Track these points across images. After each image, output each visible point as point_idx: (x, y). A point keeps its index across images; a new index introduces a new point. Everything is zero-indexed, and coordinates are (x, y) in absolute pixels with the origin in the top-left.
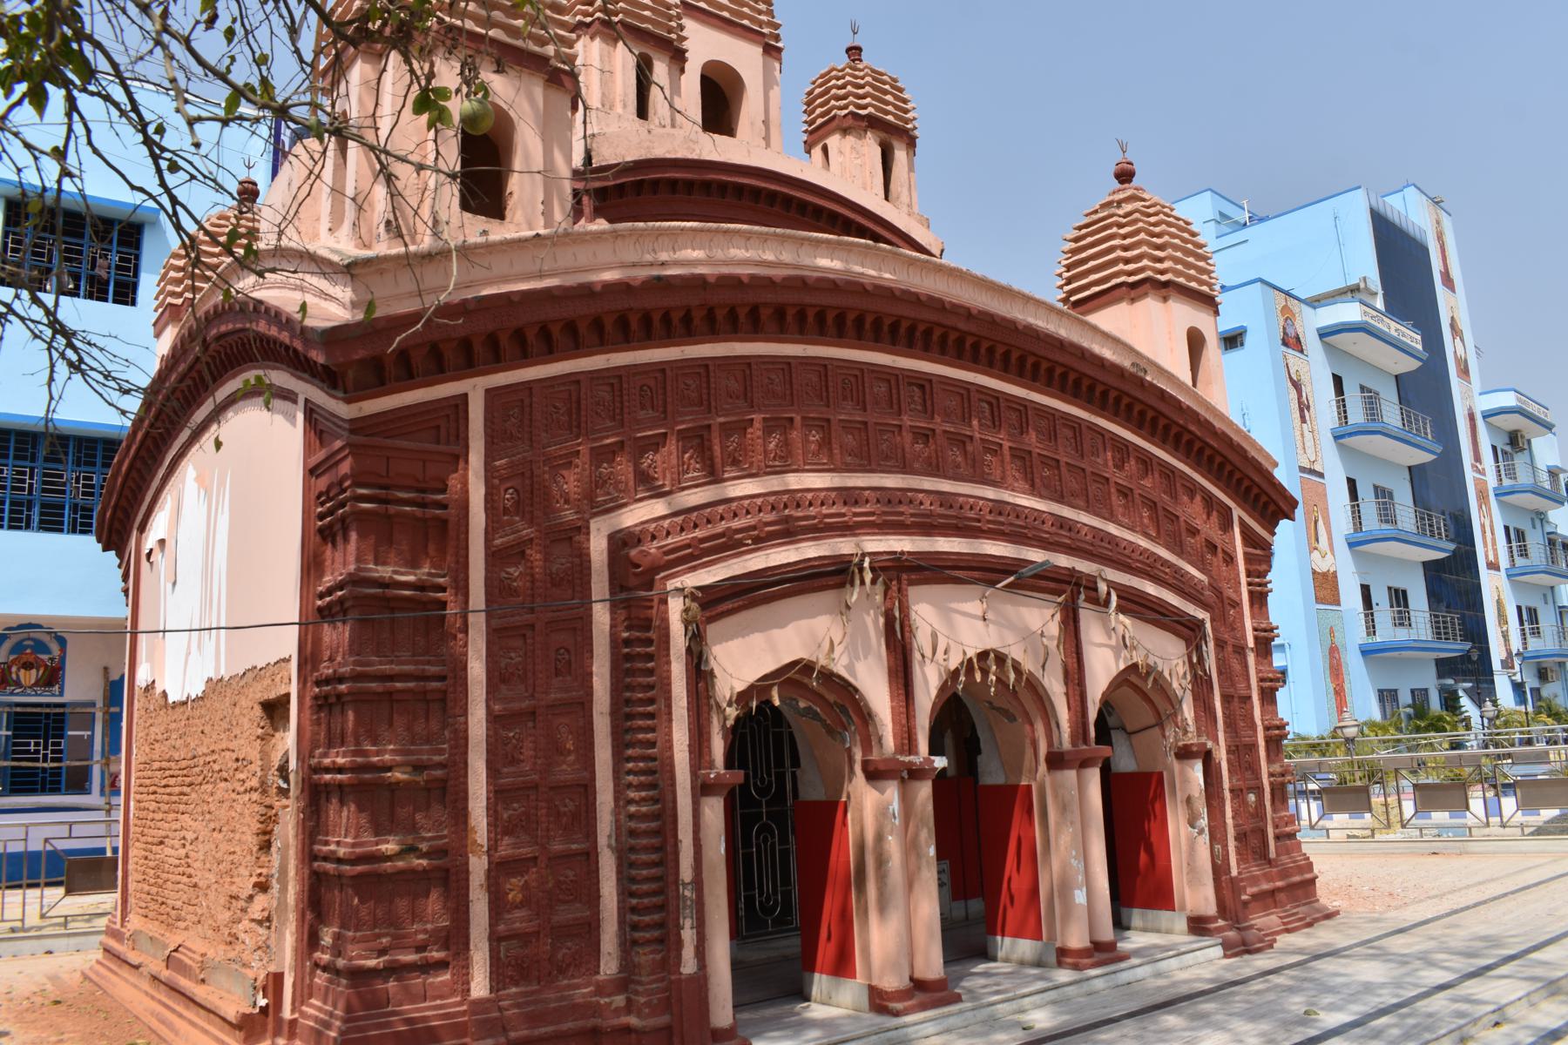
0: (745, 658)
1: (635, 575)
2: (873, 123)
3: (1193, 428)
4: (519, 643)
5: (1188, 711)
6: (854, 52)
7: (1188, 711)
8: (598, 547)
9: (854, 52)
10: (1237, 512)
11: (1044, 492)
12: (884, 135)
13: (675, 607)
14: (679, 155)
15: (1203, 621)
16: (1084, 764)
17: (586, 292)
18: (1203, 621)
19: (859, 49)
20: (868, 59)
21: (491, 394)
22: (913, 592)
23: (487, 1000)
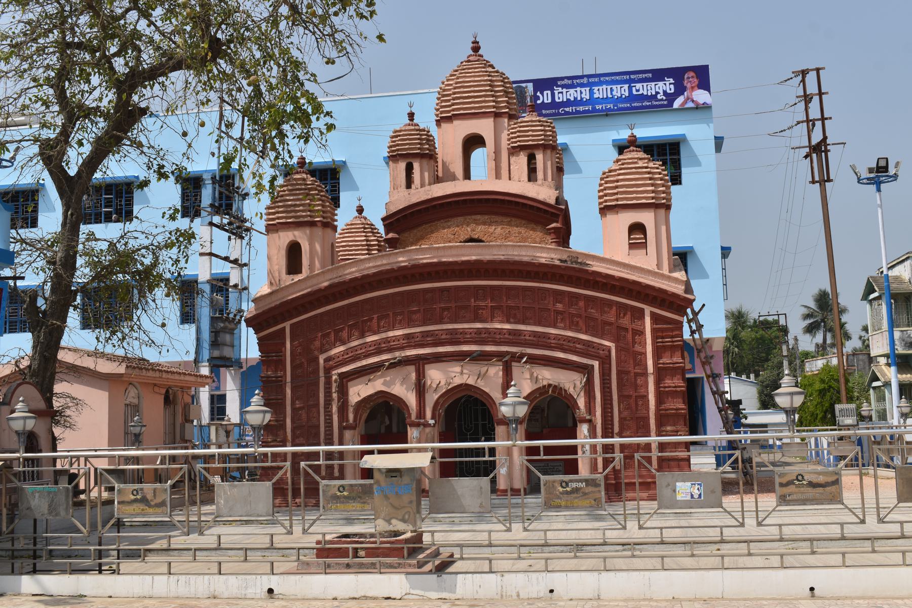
0: (359, 391)
1: (328, 371)
2: (522, 148)
3: (600, 279)
5: (581, 402)
7: (581, 402)
8: (321, 361)
10: (648, 310)
12: (529, 151)
13: (334, 377)
14: (423, 199)
17: (320, 290)
18: (593, 366)
21: (291, 325)
22: (426, 366)
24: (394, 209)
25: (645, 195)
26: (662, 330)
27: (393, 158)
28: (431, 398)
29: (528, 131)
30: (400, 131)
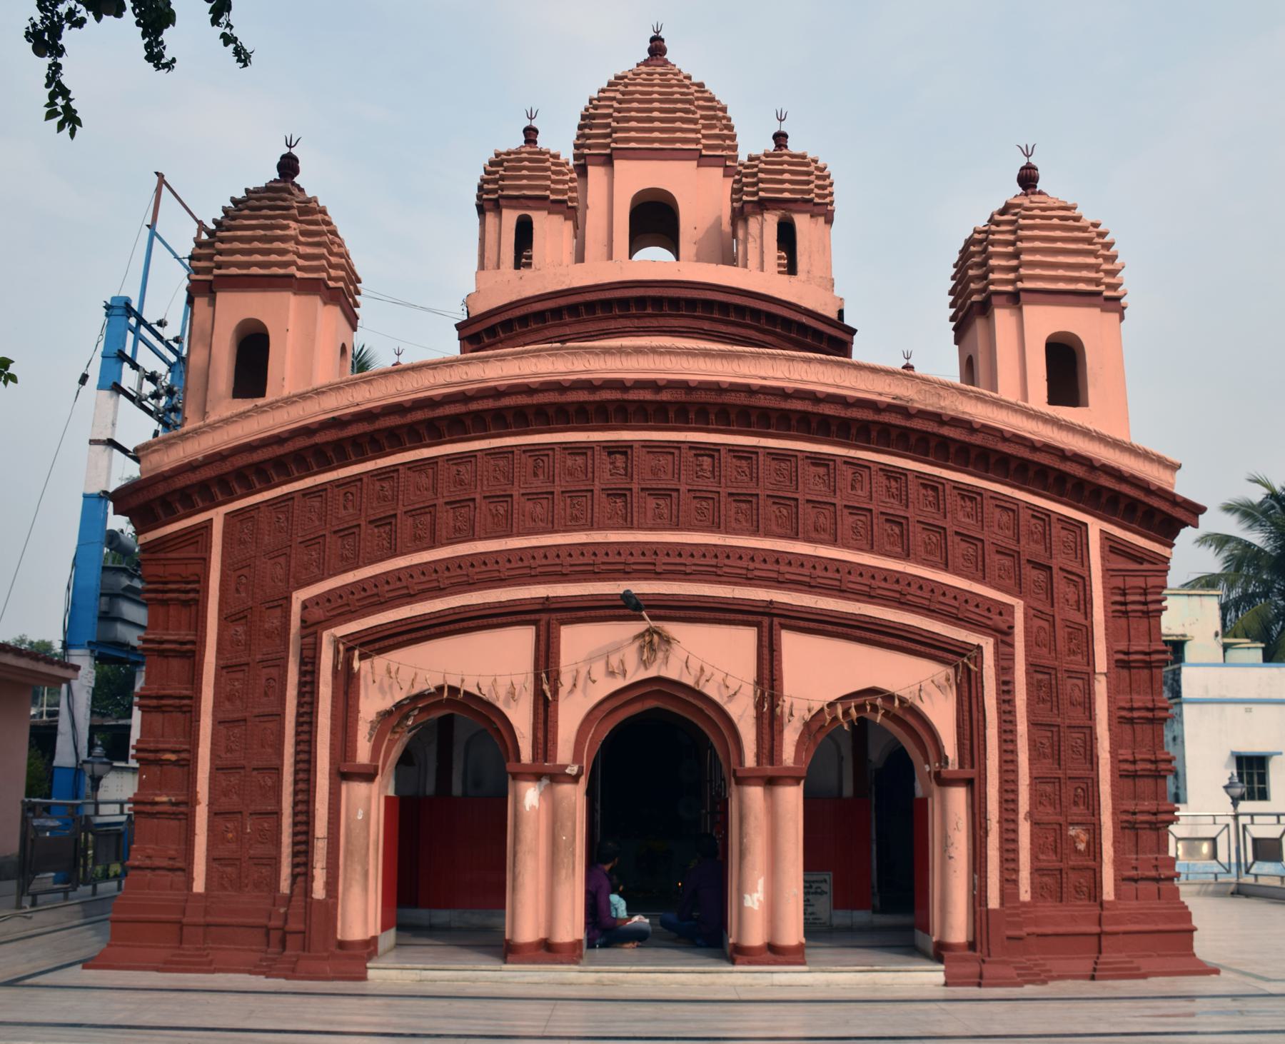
0: (388, 682)
1: (312, 629)
4: (240, 675)
6: (780, 138)
9: (780, 138)
10: (1095, 527)
11: (779, 531)
12: (779, 213)
15: (979, 648)
16: (771, 782)
19: (785, 136)
20: (794, 146)
23: (199, 894)
24: (481, 307)
25: (1085, 274)
26: (1124, 573)
27: (488, 203)
28: (571, 715)
29: (782, 172)
30: (508, 154)
